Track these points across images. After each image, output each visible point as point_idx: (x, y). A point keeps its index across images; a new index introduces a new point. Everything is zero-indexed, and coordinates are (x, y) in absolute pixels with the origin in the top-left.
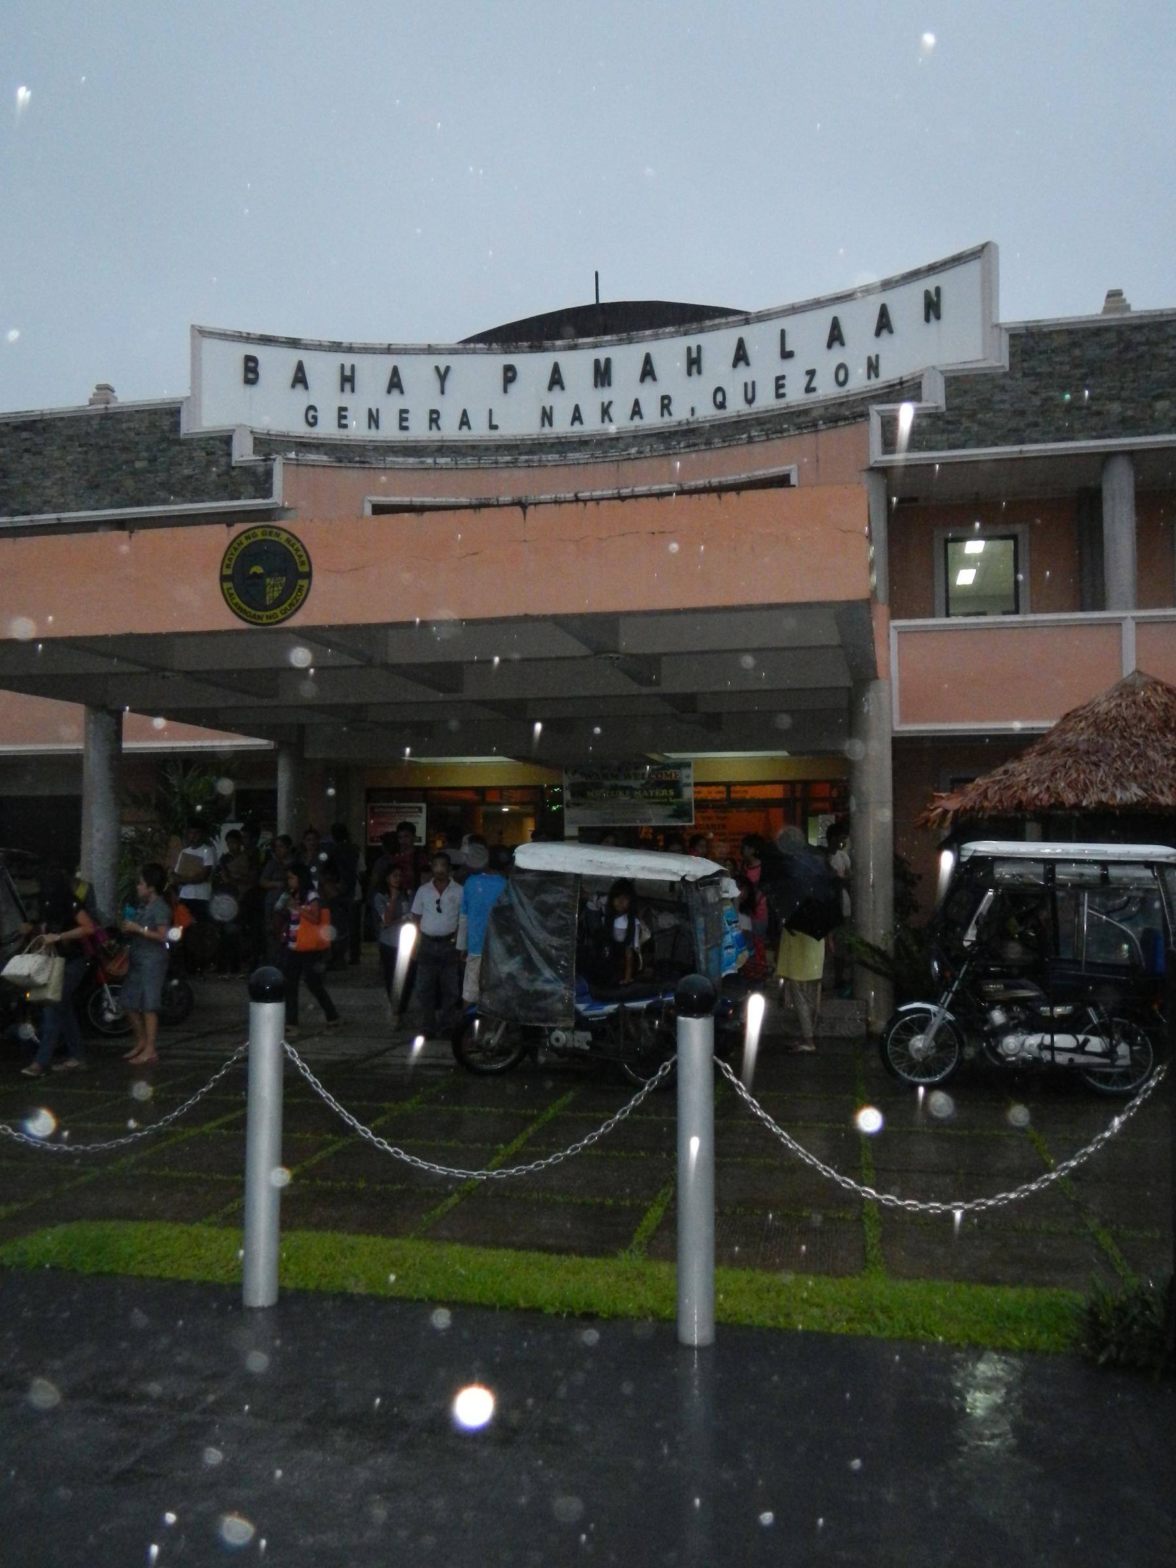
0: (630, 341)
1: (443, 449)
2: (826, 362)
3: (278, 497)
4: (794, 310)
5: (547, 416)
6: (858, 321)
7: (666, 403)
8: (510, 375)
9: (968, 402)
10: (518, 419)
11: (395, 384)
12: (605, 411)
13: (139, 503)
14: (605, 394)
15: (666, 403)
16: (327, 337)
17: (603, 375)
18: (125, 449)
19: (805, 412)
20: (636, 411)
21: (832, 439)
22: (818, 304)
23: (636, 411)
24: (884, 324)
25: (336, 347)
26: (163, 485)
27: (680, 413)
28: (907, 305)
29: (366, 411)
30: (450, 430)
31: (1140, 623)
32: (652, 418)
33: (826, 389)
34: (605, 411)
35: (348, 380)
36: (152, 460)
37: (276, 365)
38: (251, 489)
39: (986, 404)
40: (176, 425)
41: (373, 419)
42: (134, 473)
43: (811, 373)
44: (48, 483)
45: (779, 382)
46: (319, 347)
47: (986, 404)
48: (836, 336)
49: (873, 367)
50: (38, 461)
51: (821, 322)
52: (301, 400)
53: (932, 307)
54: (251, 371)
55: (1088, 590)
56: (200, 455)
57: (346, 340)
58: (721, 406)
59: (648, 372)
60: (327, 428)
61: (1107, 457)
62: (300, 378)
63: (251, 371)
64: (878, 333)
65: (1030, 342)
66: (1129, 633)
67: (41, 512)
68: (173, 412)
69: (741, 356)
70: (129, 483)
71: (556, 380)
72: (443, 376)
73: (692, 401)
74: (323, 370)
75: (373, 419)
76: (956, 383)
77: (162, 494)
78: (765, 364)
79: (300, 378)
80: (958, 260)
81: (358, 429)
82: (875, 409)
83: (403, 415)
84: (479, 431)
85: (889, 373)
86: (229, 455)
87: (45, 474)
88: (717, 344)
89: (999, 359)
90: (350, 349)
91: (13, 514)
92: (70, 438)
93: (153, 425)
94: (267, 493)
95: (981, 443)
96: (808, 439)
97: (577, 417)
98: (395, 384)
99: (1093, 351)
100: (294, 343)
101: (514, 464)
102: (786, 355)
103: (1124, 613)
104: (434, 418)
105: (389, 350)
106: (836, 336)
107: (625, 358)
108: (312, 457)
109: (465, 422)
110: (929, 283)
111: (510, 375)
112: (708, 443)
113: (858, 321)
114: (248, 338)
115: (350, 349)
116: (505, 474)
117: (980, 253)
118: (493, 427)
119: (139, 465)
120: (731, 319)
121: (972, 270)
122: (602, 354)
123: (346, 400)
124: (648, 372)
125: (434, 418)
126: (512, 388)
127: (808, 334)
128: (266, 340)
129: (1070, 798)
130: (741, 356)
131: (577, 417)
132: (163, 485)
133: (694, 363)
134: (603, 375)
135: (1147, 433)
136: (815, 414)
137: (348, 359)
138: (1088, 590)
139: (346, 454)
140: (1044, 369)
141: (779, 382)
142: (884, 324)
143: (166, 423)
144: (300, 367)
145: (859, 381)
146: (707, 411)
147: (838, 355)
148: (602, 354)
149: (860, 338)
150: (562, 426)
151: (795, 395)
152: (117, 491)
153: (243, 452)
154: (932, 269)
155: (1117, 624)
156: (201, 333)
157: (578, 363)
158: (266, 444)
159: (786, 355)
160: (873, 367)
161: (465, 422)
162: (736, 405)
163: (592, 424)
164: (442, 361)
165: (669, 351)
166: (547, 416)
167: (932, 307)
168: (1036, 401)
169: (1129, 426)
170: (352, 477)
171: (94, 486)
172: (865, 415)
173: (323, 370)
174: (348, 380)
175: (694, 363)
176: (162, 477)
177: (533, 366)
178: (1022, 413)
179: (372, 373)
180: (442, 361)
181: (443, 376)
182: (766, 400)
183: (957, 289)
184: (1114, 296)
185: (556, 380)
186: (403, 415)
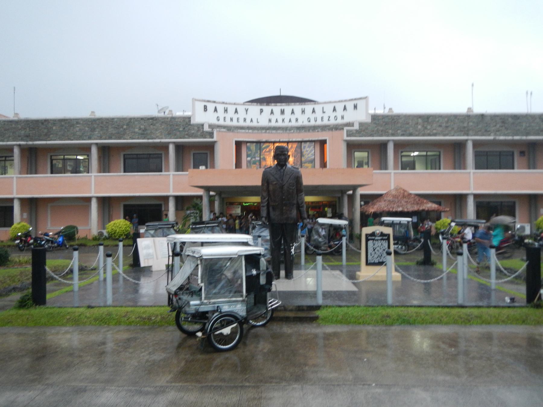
0: (289, 105)
1: (249, 128)
2: (333, 115)
3: (215, 139)
4: (325, 103)
5: (270, 121)
6: (340, 107)
7: (297, 120)
8: (262, 111)
9: (364, 128)
10: (263, 122)
11: (236, 111)
12: (283, 120)
13: (181, 138)
14: (283, 117)
15: (297, 120)
16: (221, 101)
17: (282, 112)
18: (176, 125)
19: (329, 126)
20: (290, 121)
21: (336, 133)
22: (330, 102)
23: (290, 121)
24: (345, 108)
25: (223, 103)
26: (187, 135)
27: (300, 123)
28: (350, 106)
29: (229, 119)
30: (248, 123)
31: (395, 173)
32: (294, 124)
33: (332, 122)
34: (283, 120)
35: (226, 111)
36: (184, 129)
37: (211, 107)
38: (209, 137)
39: (367, 129)
40: (190, 121)
41: (232, 120)
42: (179, 131)
43: (329, 117)
44: (157, 132)
45: (322, 118)
46: (219, 103)
47: (367, 129)
48: (334, 110)
49: (342, 117)
50: (155, 127)
51: (331, 107)
52: (216, 115)
53: (355, 107)
54: (205, 109)
55: (383, 165)
56: (196, 128)
57: (225, 101)
58: (310, 121)
59: (293, 112)
60: (221, 122)
61: (388, 141)
62: (216, 110)
63: (205, 109)
64: (344, 110)
65: (375, 117)
66: (392, 174)
67: (155, 139)
68: (189, 118)
69: (314, 111)
70: (178, 133)
71: (272, 112)
72: (247, 110)
73: (303, 121)
74: (220, 108)
75: (232, 120)
76: (361, 124)
77: (186, 136)
78: (319, 114)
79: (216, 110)
80: (361, 99)
81: (228, 123)
82: (346, 129)
83: (238, 119)
84: (255, 124)
85: (346, 120)
86: (203, 128)
87: (156, 130)
88: (309, 108)
89: (369, 120)
90: (226, 104)
91: (148, 139)
92: (163, 122)
93: (184, 121)
94: (213, 138)
95: (365, 136)
96: (330, 132)
97: (277, 121)
98: (236, 111)
99: (386, 120)
100: (214, 102)
101: (266, 132)
102: (324, 112)
103: (391, 171)
104: (245, 120)
105: (235, 104)
106: (334, 110)
107: (288, 108)
108: (223, 130)
109: (252, 121)
110: (355, 102)
111: (262, 111)
112: (309, 131)
113: (340, 107)
114: (205, 101)
115: (226, 104)
116: (264, 134)
117: (366, 98)
118: (258, 122)
119: (181, 129)
120: (312, 103)
121: (364, 101)
122: (283, 108)
123: (226, 115)
124: (293, 112)
125: (245, 120)
126: (262, 114)
127: (329, 109)
128: (209, 101)
129: (391, 210)
130: (314, 111)
131: (277, 121)
132: (187, 135)
133: (303, 112)
134: (282, 112)
135: (396, 136)
136: (331, 126)
137: (226, 106)
138: (383, 165)
139: (229, 129)
140: (377, 122)
141: (322, 118)
142: (345, 108)
143: (187, 120)
144: (216, 108)
145: (340, 121)
146: (306, 123)
147: (335, 114)
148: (283, 108)
149: (340, 111)
150: (273, 124)
151: (326, 122)
152: (175, 135)
153: (206, 128)
154: (355, 99)
155: (390, 173)
156: (194, 100)
157: (277, 108)
158: (210, 126)
159: (324, 112)
160: (342, 117)
161: (252, 121)
162: (312, 123)
163: (280, 124)
164: (247, 107)
165: (298, 108)
166: (270, 121)
167: (355, 107)
168: (376, 129)
169: (393, 135)
170: (230, 134)
171: (169, 134)
172: (343, 129)
173: (220, 108)
174: (226, 111)
175: (303, 112)
176: (186, 133)
177: (267, 109)
178: (373, 131)
179: (231, 109)
180: (247, 107)
181: (247, 110)
182: (319, 122)
183: (360, 104)
184: (390, 109)
185: (272, 112)
186: (238, 119)
